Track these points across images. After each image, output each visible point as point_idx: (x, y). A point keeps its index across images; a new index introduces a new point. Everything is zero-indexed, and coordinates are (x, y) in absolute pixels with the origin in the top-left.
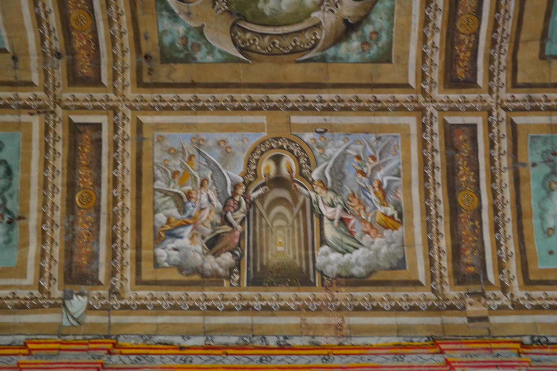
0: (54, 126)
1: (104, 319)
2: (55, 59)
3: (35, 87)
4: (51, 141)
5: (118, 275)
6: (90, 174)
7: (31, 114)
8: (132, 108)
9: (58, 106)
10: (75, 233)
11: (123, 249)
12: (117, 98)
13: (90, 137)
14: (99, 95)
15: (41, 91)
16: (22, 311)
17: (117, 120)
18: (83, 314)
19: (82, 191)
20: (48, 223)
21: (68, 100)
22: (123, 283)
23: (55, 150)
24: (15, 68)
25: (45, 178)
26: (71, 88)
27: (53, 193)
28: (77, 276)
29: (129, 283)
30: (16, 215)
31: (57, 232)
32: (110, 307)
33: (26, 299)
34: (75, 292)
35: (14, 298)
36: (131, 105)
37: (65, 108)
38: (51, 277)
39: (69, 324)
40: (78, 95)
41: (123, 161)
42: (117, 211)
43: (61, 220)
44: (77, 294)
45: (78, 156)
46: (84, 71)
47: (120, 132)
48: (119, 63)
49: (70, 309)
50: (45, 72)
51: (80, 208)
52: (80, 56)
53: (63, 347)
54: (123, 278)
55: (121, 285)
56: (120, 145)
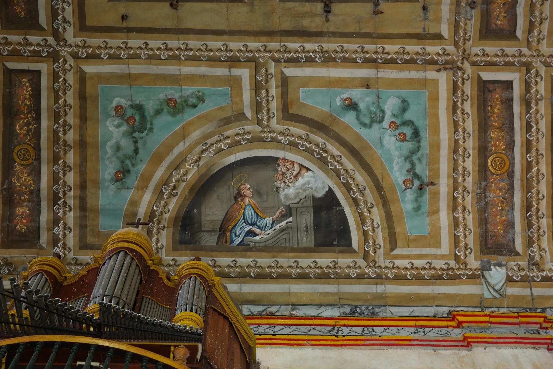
0: (463, 84)
1: (527, 292)
2: (468, 8)
3: (444, 40)
4: (460, 100)
5: (535, 245)
6: (503, 136)
7: (439, 71)
8: (546, 64)
9: (465, 62)
10: (487, 200)
11: (538, 218)
12: (530, 53)
13: (501, 96)
14: (510, 50)
15: (451, 45)
16: (439, 281)
17: (529, 77)
18: (503, 285)
19: (494, 156)
20: (460, 189)
21: (477, 55)
22: (542, 253)
23: (463, 110)
24: (425, 19)
25: (456, 141)
26: (482, 42)
27: (464, 157)
28: (494, 246)
29: (548, 253)
30: (426, 180)
31: (469, 199)
32: (530, 278)
33: (442, 269)
34: (493, 262)
35: (430, 269)
36: (545, 60)
37: (474, 64)
38: (466, 247)
39: (491, 297)
40: (488, 50)
41: (537, 124)
42: (532, 177)
43: (472, 186)
44: (495, 265)
45: (489, 117)
46: (499, 23)
47: (533, 91)
48: (537, 14)
49: (490, 281)
50: (457, 25)
51: (493, 174)
52: (496, 5)
53: (493, 320)
54: (540, 249)
55: (541, 255)
56: (532, 105)
